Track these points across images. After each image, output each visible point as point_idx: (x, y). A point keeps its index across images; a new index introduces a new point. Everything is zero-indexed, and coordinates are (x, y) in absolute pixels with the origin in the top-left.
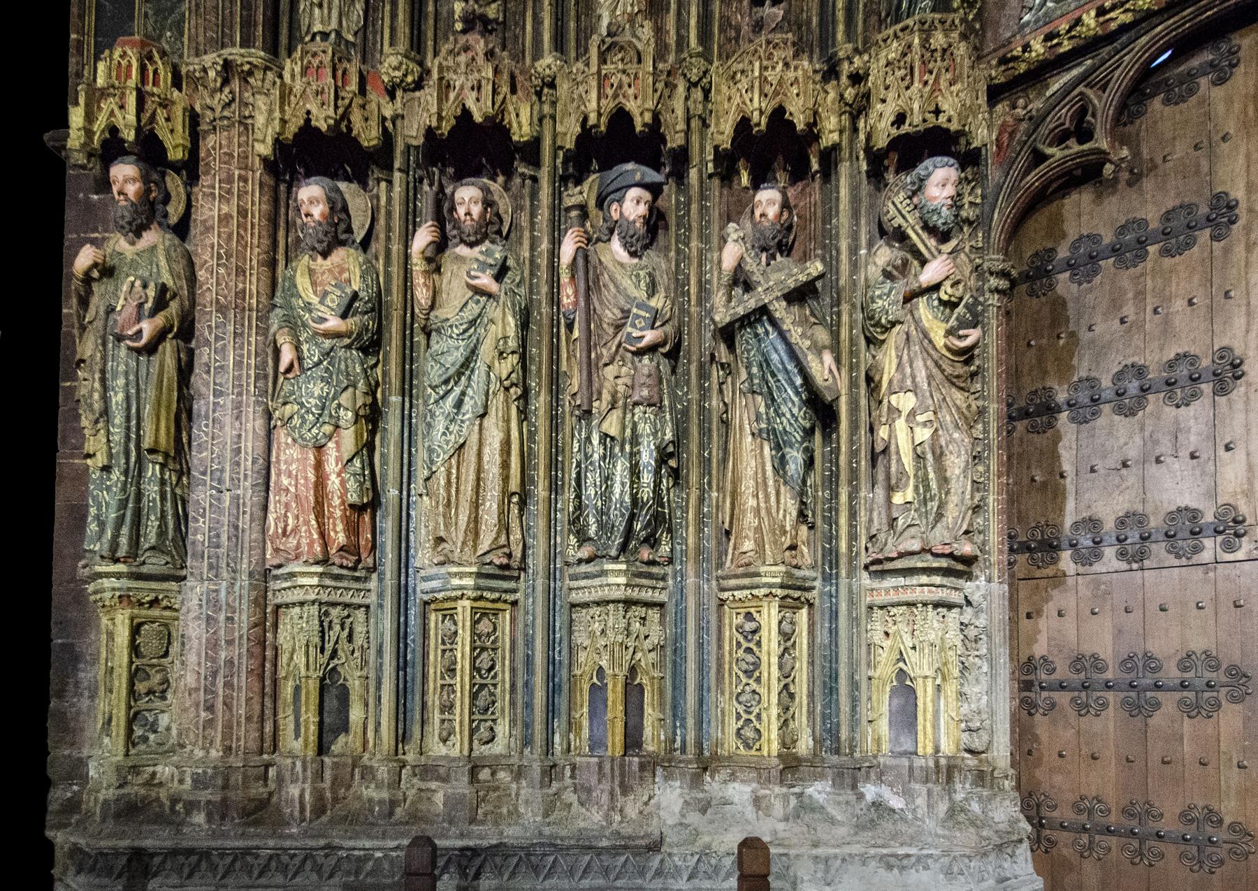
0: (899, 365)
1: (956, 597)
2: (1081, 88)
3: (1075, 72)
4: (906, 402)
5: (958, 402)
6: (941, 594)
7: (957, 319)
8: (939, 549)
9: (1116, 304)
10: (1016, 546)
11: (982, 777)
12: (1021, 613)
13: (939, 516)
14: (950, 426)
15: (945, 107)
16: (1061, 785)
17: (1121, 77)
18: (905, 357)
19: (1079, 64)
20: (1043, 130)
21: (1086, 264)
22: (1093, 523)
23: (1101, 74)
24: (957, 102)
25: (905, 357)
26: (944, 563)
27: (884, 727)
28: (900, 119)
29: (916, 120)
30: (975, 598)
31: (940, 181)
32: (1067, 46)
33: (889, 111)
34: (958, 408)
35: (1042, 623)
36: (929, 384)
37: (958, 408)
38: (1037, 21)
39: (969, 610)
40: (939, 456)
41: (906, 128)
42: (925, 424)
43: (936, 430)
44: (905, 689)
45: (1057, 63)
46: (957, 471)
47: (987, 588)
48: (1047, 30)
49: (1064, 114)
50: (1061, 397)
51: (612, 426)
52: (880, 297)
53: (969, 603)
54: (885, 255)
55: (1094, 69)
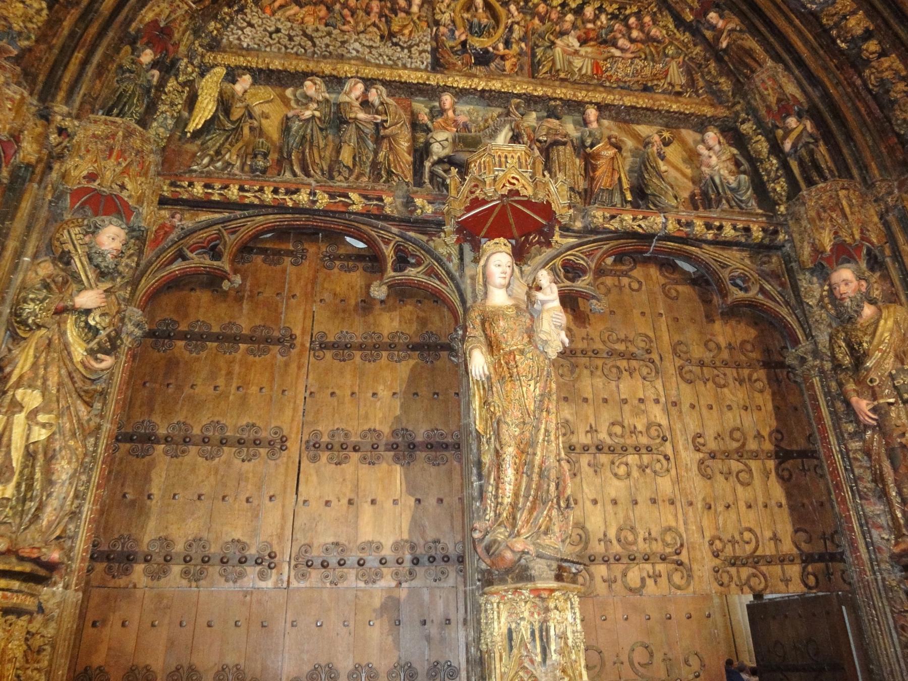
0: (35, 365)
1: (29, 603)
2: (219, 226)
3: (217, 216)
4: (32, 398)
5: (81, 414)
6: (16, 600)
7: (98, 343)
8: (26, 552)
9: (213, 375)
13: (36, 517)
14: (68, 434)
15: (129, 187)
17: (244, 234)
18: (42, 360)
19: (221, 213)
20: (192, 240)
22: (166, 542)
23: (233, 225)
25: (42, 360)
26: (27, 568)
29: (107, 183)
30: (50, 605)
32: (216, 198)
33: (86, 168)
34: (79, 420)
35: (107, 631)
36: (58, 391)
37: (79, 420)
38: (202, 172)
39: (39, 618)
40: (50, 458)
41: (95, 185)
42: (44, 426)
43: (54, 434)
46: (64, 477)
48: (207, 181)
52: (33, 300)
53: (41, 610)
55: (229, 220)
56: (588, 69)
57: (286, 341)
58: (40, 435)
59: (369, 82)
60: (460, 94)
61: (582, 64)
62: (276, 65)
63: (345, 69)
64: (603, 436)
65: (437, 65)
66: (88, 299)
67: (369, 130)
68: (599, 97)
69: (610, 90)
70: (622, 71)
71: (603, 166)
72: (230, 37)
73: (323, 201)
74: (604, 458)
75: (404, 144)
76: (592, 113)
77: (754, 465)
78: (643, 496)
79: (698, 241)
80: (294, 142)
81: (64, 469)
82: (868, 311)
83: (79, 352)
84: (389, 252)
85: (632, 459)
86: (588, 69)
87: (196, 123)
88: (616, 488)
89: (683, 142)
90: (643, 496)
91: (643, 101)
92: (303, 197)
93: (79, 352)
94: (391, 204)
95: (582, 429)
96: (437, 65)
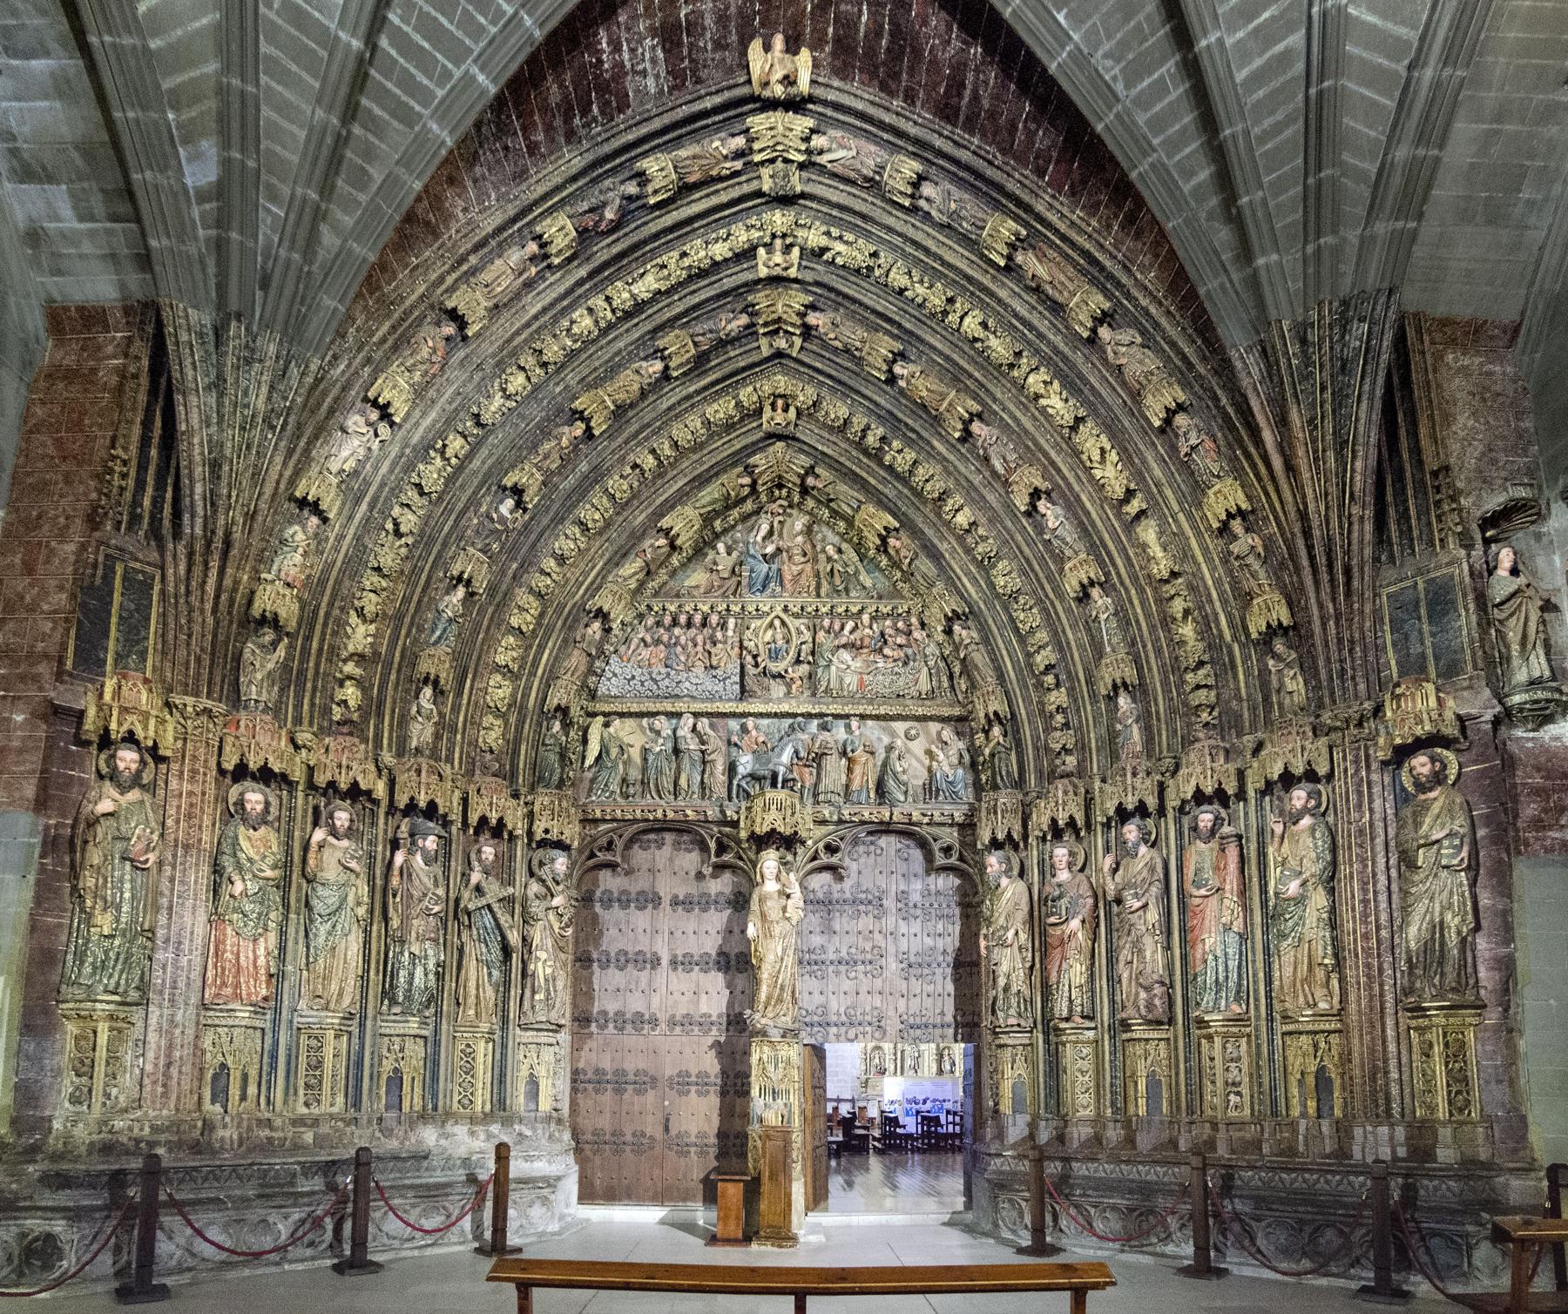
10: (575, 1019)
11: (559, 1121)
12: (576, 1048)
16: (587, 1124)
21: (608, 903)
24: (571, 832)
27: (522, 1099)
28: (547, 831)
31: (561, 863)
44: (533, 1083)
45: (604, 821)
47: (564, 1037)
49: (604, 841)
50: (595, 956)
51: (415, 949)
54: (535, 887)
56: (853, 687)
57: (656, 901)
58: (549, 971)
59: (696, 715)
60: (761, 715)
61: (851, 681)
62: (635, 708)
63: (680, 706)
64: (844, 954)
65: (744, 693)
66: (558, 901)
67: (697, 756)
68: (860, 710)
69: (871, 702)
70: (880, 683)
71: (858, 770)
72: (602, 690)
73: (671, 815)
74: (843, 968)
75: (720, 767)
76: (854, 723)
77: (939, 971)
78: (863, 990)
79: (919, 824)
80: (652, 773)
81: (560, 984)
82: (1004, 881)
83: (556, 926)
84: (713, 845)
85: (861, 968)
86: (853, 687)
87: (590, 761)
88: (848, 985)
89: (927, 733)
90: (863, 990)
91: (893, 711)
92: (659, 814)
93: (556, 926)
94: (713, 813)
95: (831, 949)
96: (744, 693)
